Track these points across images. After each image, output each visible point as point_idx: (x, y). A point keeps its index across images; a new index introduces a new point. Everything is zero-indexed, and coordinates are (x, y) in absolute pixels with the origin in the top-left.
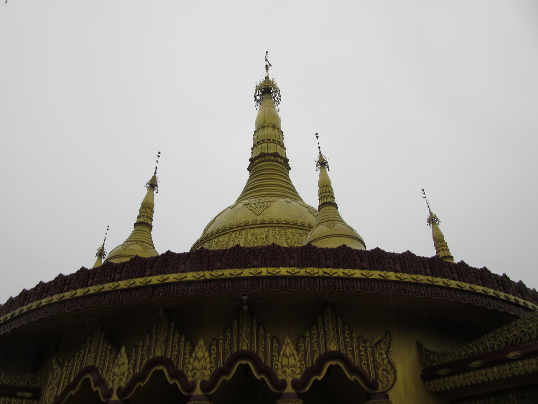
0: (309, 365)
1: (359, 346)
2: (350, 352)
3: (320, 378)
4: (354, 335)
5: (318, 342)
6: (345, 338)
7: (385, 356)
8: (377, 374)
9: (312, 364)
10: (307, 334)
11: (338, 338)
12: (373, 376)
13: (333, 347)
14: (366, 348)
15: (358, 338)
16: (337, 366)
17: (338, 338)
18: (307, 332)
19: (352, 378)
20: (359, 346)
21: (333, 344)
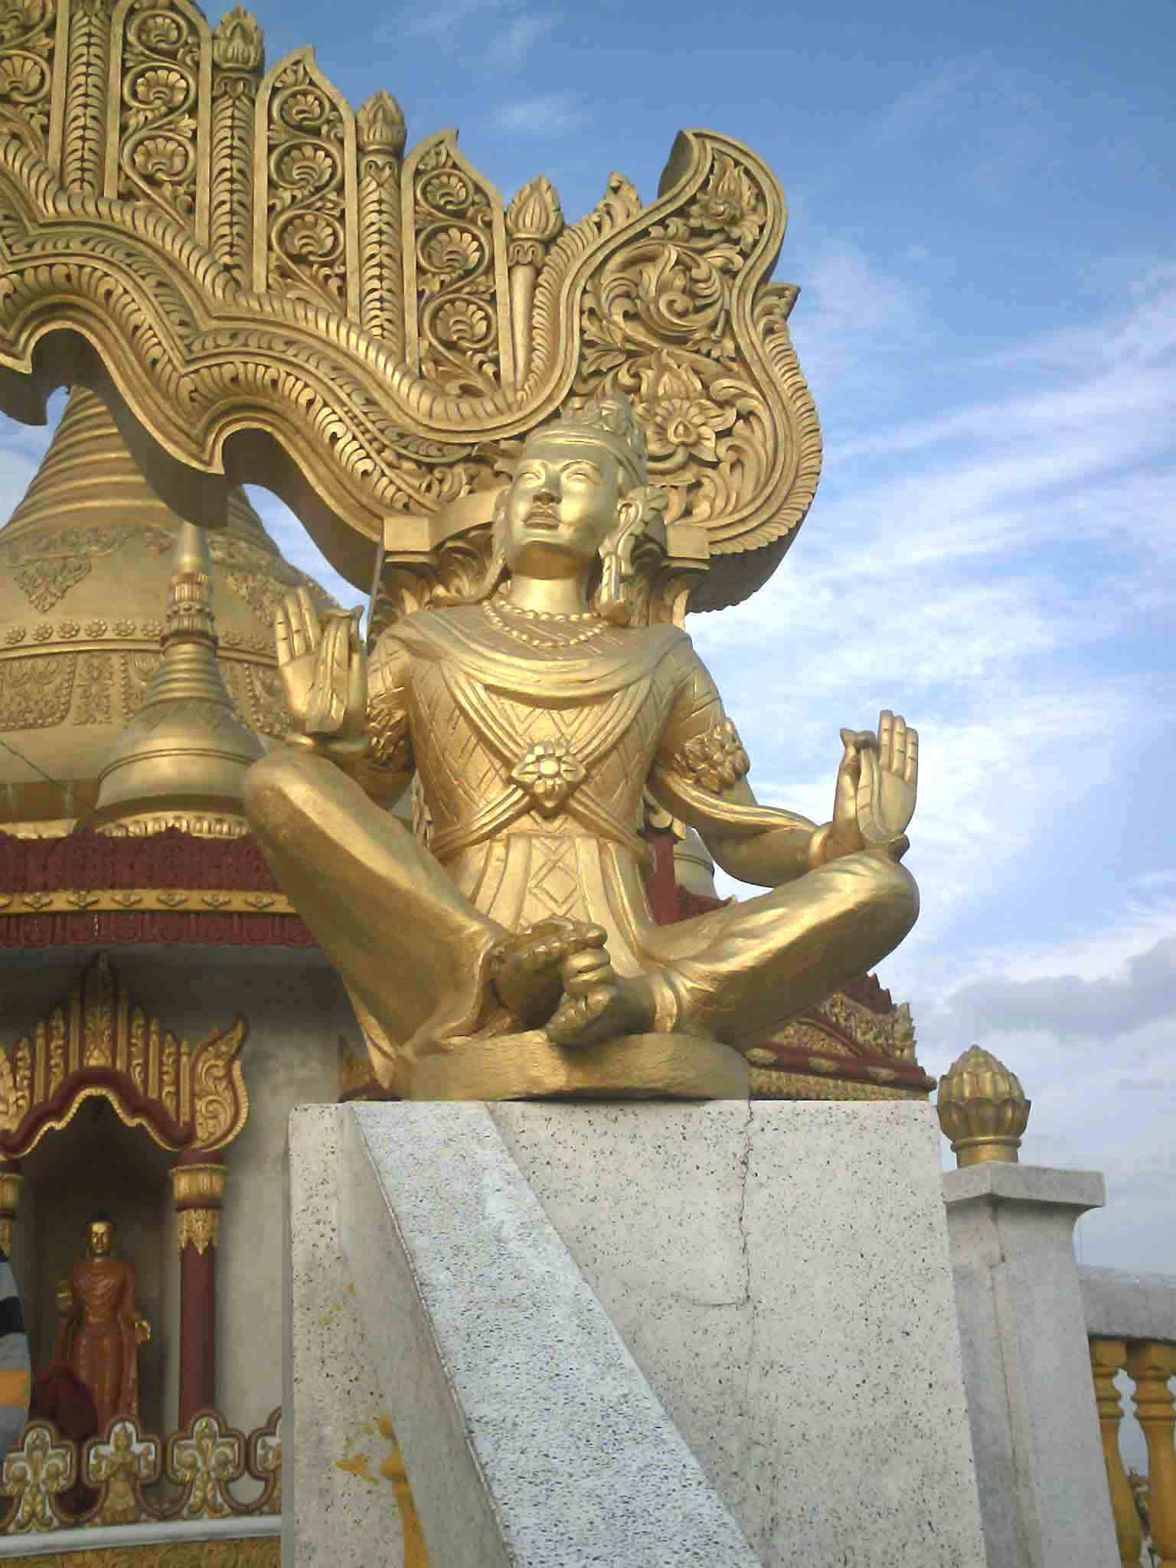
0: (39, 1099)
1: (161, 1051)
2: (138, 1069)
3: (59, 1126)
4: (153, 1028)
5: (66, 1048)
6: (130, 1036)
7: (220, 1073)
8: (193, 1111)
9: (46, 1094)
10: (40, 1031)
11: (113, 1039)
12: (185, 1118)
13: (96, 1059)
14: (178, 1055)
15: (162, 1034)
16: (102, 1101)
17: (113, 1039)
18: (41, 1024)
19: (132, 1122)
20: (161, 1051)
21: (96, 1053)
